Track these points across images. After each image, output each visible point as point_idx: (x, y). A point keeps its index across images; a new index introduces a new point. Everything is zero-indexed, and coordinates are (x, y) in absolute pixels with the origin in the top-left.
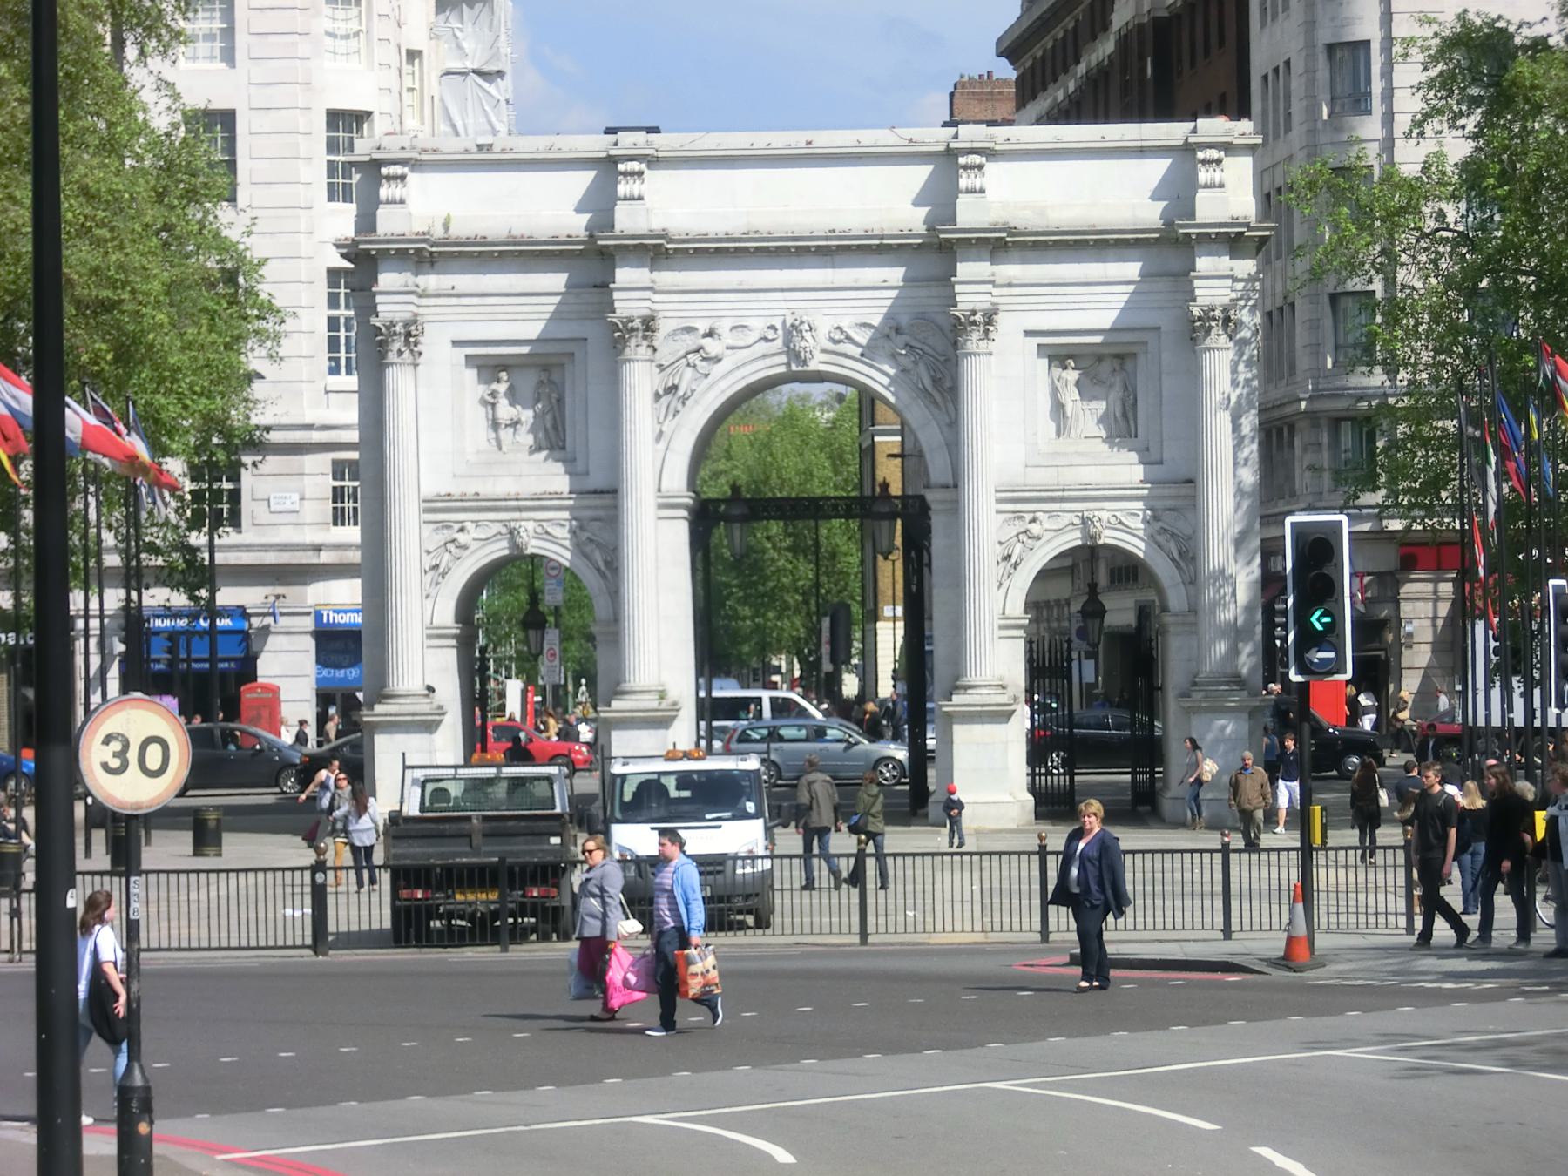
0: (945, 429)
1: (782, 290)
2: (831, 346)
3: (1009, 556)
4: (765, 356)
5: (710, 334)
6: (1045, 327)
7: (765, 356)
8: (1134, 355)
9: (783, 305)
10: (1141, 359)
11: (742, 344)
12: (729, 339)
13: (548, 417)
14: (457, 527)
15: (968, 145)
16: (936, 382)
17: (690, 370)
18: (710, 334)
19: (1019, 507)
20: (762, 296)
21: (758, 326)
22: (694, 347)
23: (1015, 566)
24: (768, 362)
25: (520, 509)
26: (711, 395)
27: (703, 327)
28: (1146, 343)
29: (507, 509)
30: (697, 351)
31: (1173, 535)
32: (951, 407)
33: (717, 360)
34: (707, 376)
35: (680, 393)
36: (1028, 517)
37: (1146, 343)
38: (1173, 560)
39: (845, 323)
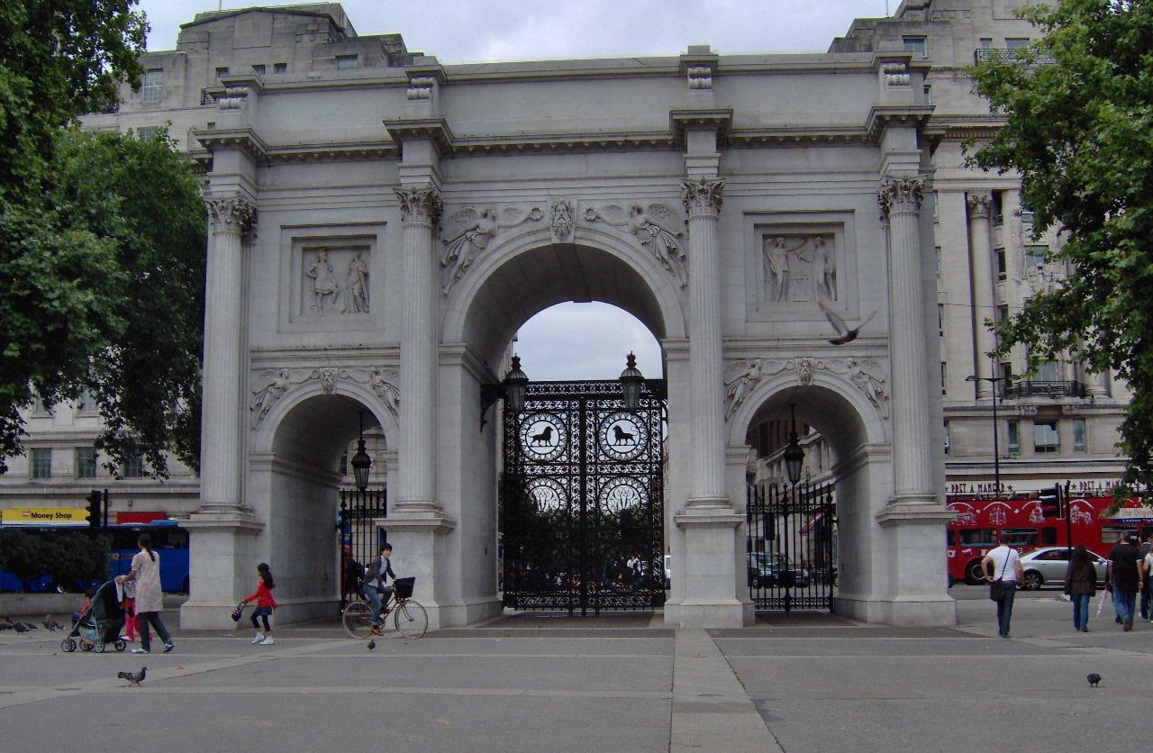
0: (679, 291)
1: (545, 180)
2: (584, 224)
3: (733, 396)
4: (529, 233)
5: (485, 216)
6: (761, 208)
7: (529, 233)
8: (832, 236)
9: (545, 192)
10: (838, 237)
11: (508, 223)
12: (501, 222)
13: (357, 287)
14: (278, 372)
15: (697, 59)
16: (671, 251)
17: (467, 243)
18: (485, 216)
19: (740, 355)
20: (528, 185)
21: (526, 209)
22: (472, 226)
23: (738, 404)
24: (533, 238)
25: (328, 358)
26: (486, 265)
27: (480, 210)
28: (842, 224)
29: (318, 358)
30: (475, 229)
31: (870, 378)
32: (684, 276)
33: (490, 236)
34: (483, 249)
35: (459, 262)
36: (749, 363)
37: (842, 224)
38: (871, 399)
39: (597, 206)
